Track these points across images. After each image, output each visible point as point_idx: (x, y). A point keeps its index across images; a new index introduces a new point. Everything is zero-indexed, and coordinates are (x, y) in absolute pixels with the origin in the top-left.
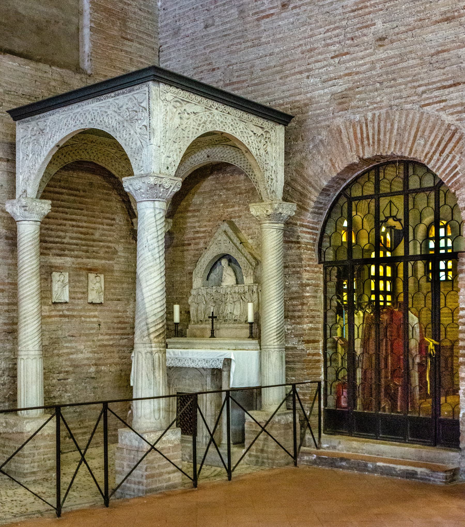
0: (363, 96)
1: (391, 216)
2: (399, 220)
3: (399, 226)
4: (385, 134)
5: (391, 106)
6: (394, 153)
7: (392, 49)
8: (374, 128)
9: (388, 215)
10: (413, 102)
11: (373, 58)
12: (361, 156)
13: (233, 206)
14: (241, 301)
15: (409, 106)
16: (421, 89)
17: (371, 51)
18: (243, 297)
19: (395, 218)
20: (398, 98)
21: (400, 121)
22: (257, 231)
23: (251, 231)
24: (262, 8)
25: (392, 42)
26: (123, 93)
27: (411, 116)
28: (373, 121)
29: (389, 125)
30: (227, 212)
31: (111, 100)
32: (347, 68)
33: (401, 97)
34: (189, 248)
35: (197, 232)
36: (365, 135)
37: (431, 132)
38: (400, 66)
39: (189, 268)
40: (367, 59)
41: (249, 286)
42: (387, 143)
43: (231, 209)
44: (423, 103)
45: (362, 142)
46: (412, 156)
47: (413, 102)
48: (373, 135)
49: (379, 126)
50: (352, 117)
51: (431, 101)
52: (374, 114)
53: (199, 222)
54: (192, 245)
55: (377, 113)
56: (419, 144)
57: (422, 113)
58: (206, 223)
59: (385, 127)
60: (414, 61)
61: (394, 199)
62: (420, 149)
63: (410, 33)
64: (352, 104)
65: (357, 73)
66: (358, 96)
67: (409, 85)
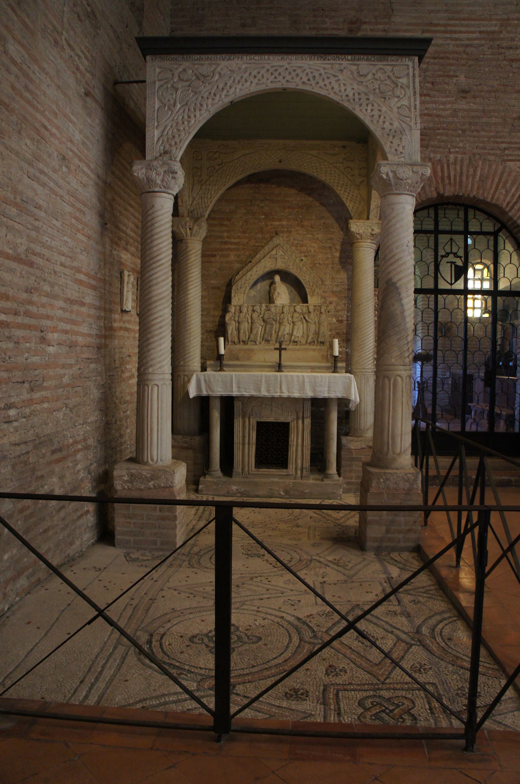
0: (445, 138)
1: (451, 253)
2: (460, 257)
3: (460, 263)
4: (467, 178)
5: (474, 155)
6: (477, 196)
7: (474, 103)
8: (455, 169)
9: (449, 251)
10: (496, 155)
11: (455, 106)
12: (442, 192)
13: (280, 220)
14: (304, 321)
15: (492, 158)
16: (504, 145)
17: (453, 99)
18: (307, 318)
19: (456, 255)
20: (482, 149)
21: (482, 169)
22: (312, 250)
23: (304, 249)
24: (325, 26)
25: (475, 97)
26: (367, 60)
27: (494, 167)
28: (455, 163)
29: (471, 170)
30: (271, 225)
31: (345, 63)
32: (426, 109)
33: (485, 149)
34: (213, 259)
35: (226, 243)
36: (446, 174)
37: (512, 185)
38: (484, 120)
39: (213, 282)
40: (449, 106)
41: (315, 306)
42: (470, 186)
43: (278, 223)
44: (506, 158)
45: (443, 179)
46: (494, 201)
47: (496, 155)
48: (455, 176)
49: (461, 169)
50: (432, 155)
51: (514, 158)
52: (456, 158)
53: (228, 232)
54: (218, 257)
55: (459, 157)
56: (501, 193)
57: (505, 167)
58: (239, 234)
59: (468, 171)
60: (497, 120)
61: (455, 237)
62: (502, 197)
63: (493, 94)
64: (432, 143)
65: (438, 116)
66: (439, 137)
67: (492, 139)
